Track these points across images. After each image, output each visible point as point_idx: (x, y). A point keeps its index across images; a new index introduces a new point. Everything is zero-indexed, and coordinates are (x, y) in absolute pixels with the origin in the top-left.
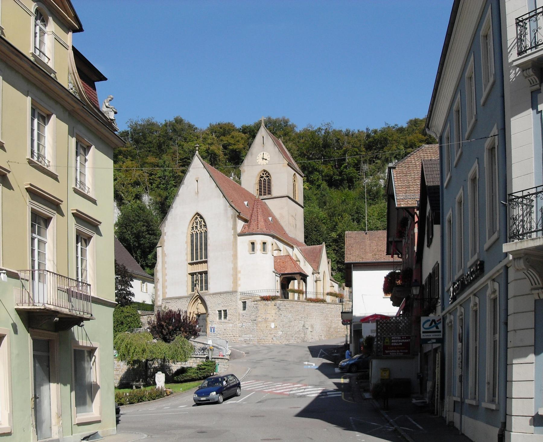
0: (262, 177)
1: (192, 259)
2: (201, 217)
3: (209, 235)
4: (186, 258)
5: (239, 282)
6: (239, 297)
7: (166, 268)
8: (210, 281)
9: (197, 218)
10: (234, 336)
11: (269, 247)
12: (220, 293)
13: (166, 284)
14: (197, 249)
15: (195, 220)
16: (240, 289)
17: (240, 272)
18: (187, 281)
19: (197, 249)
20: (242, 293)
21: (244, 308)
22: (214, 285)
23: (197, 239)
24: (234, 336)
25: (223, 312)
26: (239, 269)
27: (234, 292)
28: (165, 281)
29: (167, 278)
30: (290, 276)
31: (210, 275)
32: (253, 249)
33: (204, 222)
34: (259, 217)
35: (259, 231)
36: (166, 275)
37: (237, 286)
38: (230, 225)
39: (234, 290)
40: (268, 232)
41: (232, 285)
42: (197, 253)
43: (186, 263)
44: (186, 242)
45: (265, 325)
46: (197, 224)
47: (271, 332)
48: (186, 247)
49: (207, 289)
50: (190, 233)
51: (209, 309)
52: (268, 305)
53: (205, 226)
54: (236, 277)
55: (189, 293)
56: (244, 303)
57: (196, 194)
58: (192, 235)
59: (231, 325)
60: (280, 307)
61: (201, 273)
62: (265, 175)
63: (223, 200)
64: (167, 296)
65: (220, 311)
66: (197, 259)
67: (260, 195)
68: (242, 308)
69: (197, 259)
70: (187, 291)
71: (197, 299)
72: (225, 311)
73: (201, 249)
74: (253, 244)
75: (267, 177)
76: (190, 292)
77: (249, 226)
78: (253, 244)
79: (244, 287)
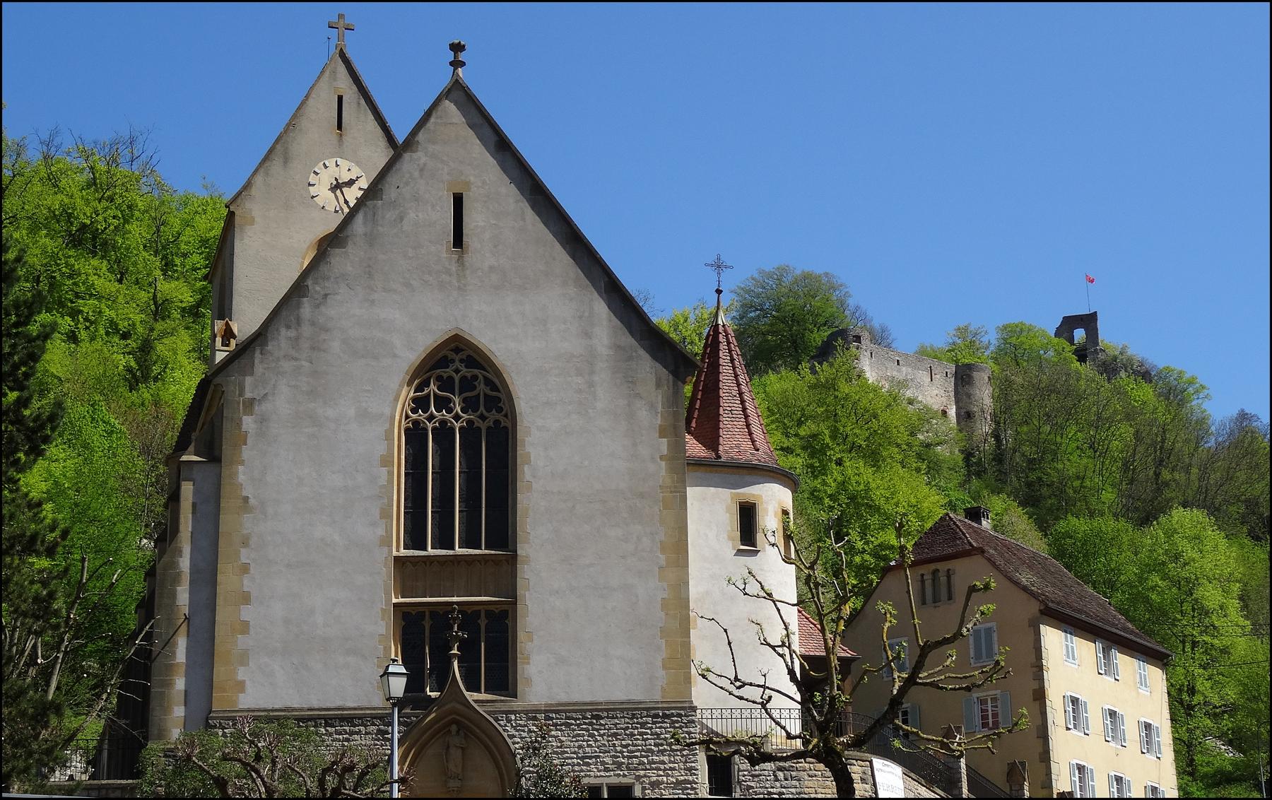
4: (381, 531)
44: (386, 461)
66: (444, 540)
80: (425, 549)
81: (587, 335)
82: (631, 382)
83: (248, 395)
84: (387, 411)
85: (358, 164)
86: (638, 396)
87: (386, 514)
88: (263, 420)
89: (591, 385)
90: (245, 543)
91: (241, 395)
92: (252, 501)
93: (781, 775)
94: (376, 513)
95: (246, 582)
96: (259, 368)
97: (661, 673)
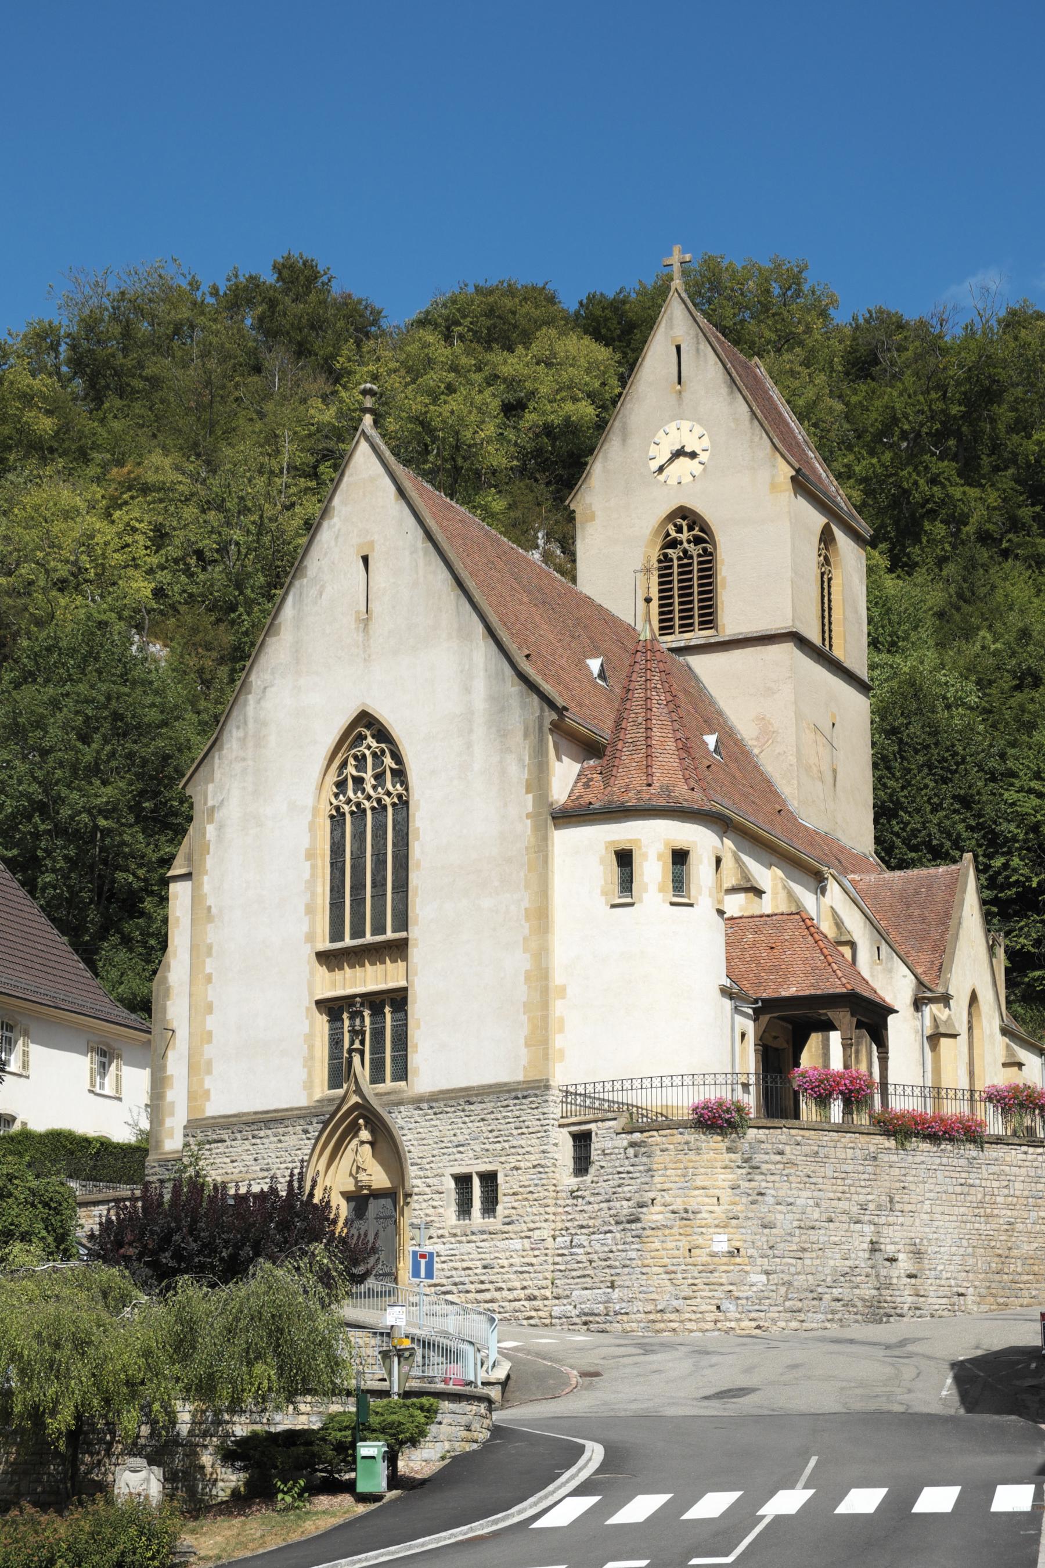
0: (674, 544)
1: (336, 934)
2: (383, 735)
3: (420, 819)
4: (305, 928)
5: (558, 1041)
6: (555, 1110)
7: (209, 979)
8: (417, 1035)
9: (361, 738)
10: (532, 1298)
11: (701, 869)
13: (209, 1051)
14: (358, 887)
15: (353, 745)
16: (561, 1076)
17: (562, 991)
18: (309, 1038)
19: (358, 887)
21: (582, 1164)
22: (440, 1055)
23: (359, 836)
24: (532, 1298)
25: (476, 1182)
26: (558, 977)
28: (202, 1037)
29: (211, 1022)
31: (417, 1009)
32: (627, 884)
33: (397, 757)
34: (656, 733)
35: (653, 796)
36: (210, 1008)
37: (546, 1057)
38: (518, 772)
40: (697, 800)
42: (358, 902)
43: (307, 954)
44: (310, 855)
45: (684, 1244)
46: (360, 760)
47: (714, 1278)
48: (307, 875)
49: (402, 1073)
50: (326, 810)
51: (412, 1171)
53: (400, 774)
54: (545, 1019)
55: (318, 1096)
56: (582, 1140)
57: (358, 620)
58: (337, 819)
59: (517, 1244)
60: (759, 1158)
61: (375, 1001)
62: (684, 536)
63: (482, 651)
64: (215, 1108)
65: (463, 1181)
66: (358, 932)
67: (666, 628)
68: (570, 1164)
69: (358, 932)
70: (309, 1085)
72: (489, 1179)
73: (379, 884)
74: (624, 858)
75: (697, 541)
76: (321, 1090)
77: (607, 775)
78: (624, 858)
80: (342, 939)
81: (467, 690)
82: (503, 734)
83: (210, 803)
85: (699, 421)
86: (508, 750)
87: (310, 910)
88: (221, 828)
89: (469, 745)
90: (209, 954)
91: (205, 803)
92: (214, 910)
93: (631, 1152)
94: (302, 909)
95: (210, 992)
96: (217, 775)
97: (524, 1051)
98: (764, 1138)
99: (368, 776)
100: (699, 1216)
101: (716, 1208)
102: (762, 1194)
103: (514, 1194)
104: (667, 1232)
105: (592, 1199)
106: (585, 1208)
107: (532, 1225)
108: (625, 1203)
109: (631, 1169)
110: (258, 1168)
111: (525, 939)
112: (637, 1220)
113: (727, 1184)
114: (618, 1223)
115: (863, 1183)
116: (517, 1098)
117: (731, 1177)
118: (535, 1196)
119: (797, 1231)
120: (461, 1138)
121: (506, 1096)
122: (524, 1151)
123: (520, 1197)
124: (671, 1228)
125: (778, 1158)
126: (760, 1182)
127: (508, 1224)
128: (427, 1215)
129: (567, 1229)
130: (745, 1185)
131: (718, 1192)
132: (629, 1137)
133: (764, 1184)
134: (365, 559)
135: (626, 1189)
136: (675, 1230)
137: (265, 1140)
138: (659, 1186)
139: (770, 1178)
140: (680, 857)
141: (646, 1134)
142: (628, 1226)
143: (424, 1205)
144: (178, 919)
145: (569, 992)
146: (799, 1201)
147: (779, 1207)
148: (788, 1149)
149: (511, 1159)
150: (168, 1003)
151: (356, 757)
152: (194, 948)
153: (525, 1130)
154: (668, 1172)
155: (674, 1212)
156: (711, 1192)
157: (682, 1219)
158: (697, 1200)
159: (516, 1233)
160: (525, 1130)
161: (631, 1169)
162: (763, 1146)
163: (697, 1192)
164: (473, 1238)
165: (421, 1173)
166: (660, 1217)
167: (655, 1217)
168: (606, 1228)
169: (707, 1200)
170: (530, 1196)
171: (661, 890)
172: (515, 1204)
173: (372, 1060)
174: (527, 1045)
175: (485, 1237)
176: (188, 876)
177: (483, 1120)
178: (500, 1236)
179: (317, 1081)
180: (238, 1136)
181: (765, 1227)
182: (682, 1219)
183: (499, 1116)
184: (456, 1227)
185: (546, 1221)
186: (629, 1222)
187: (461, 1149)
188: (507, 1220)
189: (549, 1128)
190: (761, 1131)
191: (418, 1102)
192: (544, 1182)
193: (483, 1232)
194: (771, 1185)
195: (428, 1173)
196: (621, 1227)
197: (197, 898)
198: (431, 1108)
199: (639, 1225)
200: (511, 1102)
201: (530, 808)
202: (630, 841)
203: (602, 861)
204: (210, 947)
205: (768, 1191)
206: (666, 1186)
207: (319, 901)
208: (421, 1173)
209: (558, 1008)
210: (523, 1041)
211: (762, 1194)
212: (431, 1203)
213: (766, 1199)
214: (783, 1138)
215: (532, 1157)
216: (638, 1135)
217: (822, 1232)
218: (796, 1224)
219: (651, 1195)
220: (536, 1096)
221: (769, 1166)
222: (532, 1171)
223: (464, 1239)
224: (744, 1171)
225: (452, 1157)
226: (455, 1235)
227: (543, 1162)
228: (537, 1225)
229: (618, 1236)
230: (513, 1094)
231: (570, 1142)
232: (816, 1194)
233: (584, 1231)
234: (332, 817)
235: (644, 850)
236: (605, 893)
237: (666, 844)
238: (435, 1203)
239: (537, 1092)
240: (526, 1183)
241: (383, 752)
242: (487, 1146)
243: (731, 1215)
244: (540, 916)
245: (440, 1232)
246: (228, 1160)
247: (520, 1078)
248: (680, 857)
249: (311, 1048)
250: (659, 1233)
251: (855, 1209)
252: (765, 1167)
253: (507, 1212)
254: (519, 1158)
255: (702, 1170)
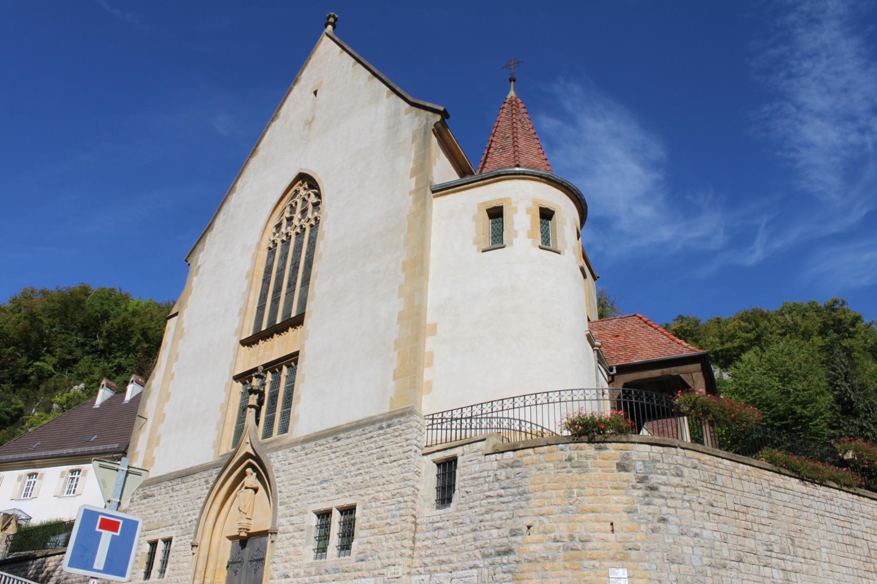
5: (427, 375)
8: (301, 389)
9: (297, 192)
12: (335, 433)
14: (277, 290)
16: (428, 405)
19: (277, 290)
20: (437, 420)
21: (445, 493)
23: (284, 257)
26: (430, 318)
27: (398, 416)
30: (657, 373)
32: (497, 239)
34: (522, 142)
36: (168, 398)
38: (406, 163)
39: (400, 406)
41: (391, 385)
43: (236, 341)
46: (293, 209)
48: (244, 289)
50: (266, 244)
52: (582, 468)
58: (272, 251)
60: (654, 479)
61: (273, 367)
65: (324, 515)
71: (243, 475)
73: (292, 284)
74: (496, 213)
78: (496, 213)
79: (449, 386)
84: (256, 241)
92: (185, 331)
93: (502, 474)
98: (658, 457)
99: (297, 215)
100: (589, 545)
101: (611, 536)
102: (663, 520)
103: (371, 527)
104: (548, 565)
105: (455, 531)
106: (447, 541)
107: (386, 561)
108: (495, 532)
109: (502, 492)
110: (169, 517)
111: (401, 287)
112: (508, 552)
113: (621, 507)
114: (485, 556)
115: (763, 521)
116: (381, 428)
117: (625, 498)
118: (392, 528)
119: (709, 571)
120: (325, 475)
121: (371, 428)
122: (383, 480)
123: (376, 530)
124: (554, 559)
125: (677, 480)
126: (659, 506)
127: (362, 560)
128: (287, 553)
129: (426, 565)
130: (642, 509)
131: (610, 517)
132: (499, 456)
133: (665, 510)
134: (315, 93)
135: (496, 515)
136: (559, 563)
137: (179, 493)
138: (536, 510)
139: (671, 502)
140: (546, 215)
141: (519, 453)
142: (498, 559)
143: (286, 543)
144: (166, 344)
145: (440, 330)
146: (705, 533)
147: (685, 538)
148: (686, 471)
149: (370, 491)
150: (148, 401)
151: (291, 206)
152: (170, 357)
153: (387, 460)
154: (546, 494)
155: (556, 540)
156: (603, 516)
157: (566, 549)
158: (585, 525)
159: (369, 570)
160: (387, 460)
161: (502, 492)
162: (658, 465)
163: (584, 517)
164: (327, 577)
165: (287, 512)
166: (538, 547)
167: (532, 548)
168: (471, 563)
169: (597, 526)
170: (387, 529)
171: (530, 235)
172: (371, 539)
173: (266, 419)
174: (395, 378)
175: (337, 575)
176: (176, 314)
177: (347, 454)
178: (354, 574)
179: (224, 441)
180: (163, 491)
181: (673, 562)
182: (566, 549)
183: (363, 449)
184: (312, 565)
185: (402, 555)
186: (499, 554)
187: (325, 485)
188: (361, 556)
189: (412, 454)
190: (654, 448)
191: (291, 445)
192: (403, 512)
193: (336, 570)
194: (672, 511)
195: (294, 512)
196: (488, 561)
197: (178, 325)
198: (304, 448)
199: (512, 557)
200: (375, 434)
201: (413, 187)
202: (501, 199)
203: (475, 219)
204: (177, 355)
205: (671, 518)
206: (544, 510)
207: (250, 306)
208: (287, 512)
209: (430, 344)
210: (392, 375)
211: (663, 520)
212: (292, 541)
213: (670, 527)
214: (679, 459)
215: (392, 487)
216: (511, 454)
217: (734, 573)
218: (706, 560)
219: (528, 521)
220: (400, 423)
221: (669, 489)
222: (390, 502)
223: (318, 578)
224: (640, 493)
225: (316, 494)
226: (309, 574)
227: (402, 491)
228: (392, 561)
229: (486, 571)
230: (378, 425)
231: (434, 470)
232: (721, 526)
233: (444, 567)
234: (270, 249)
235: (514, 205)
236: (476, 242)
237: (534, 201)
238: (296, 541)
239: (402, 419)
240: (384, 515)
241: (309, 195)
242: (349, 480)
243: (630, 545)
244: (417, 266)
245: (296, 571)
246: (153, 511)
247: (386, 409)
248: (546, 215)
249: (225, 414)
250: (539, 567)
251: (761, 549)
252: (663, 489)
253: (361, 547)
254: (379, 488)
255: (590, 490)
